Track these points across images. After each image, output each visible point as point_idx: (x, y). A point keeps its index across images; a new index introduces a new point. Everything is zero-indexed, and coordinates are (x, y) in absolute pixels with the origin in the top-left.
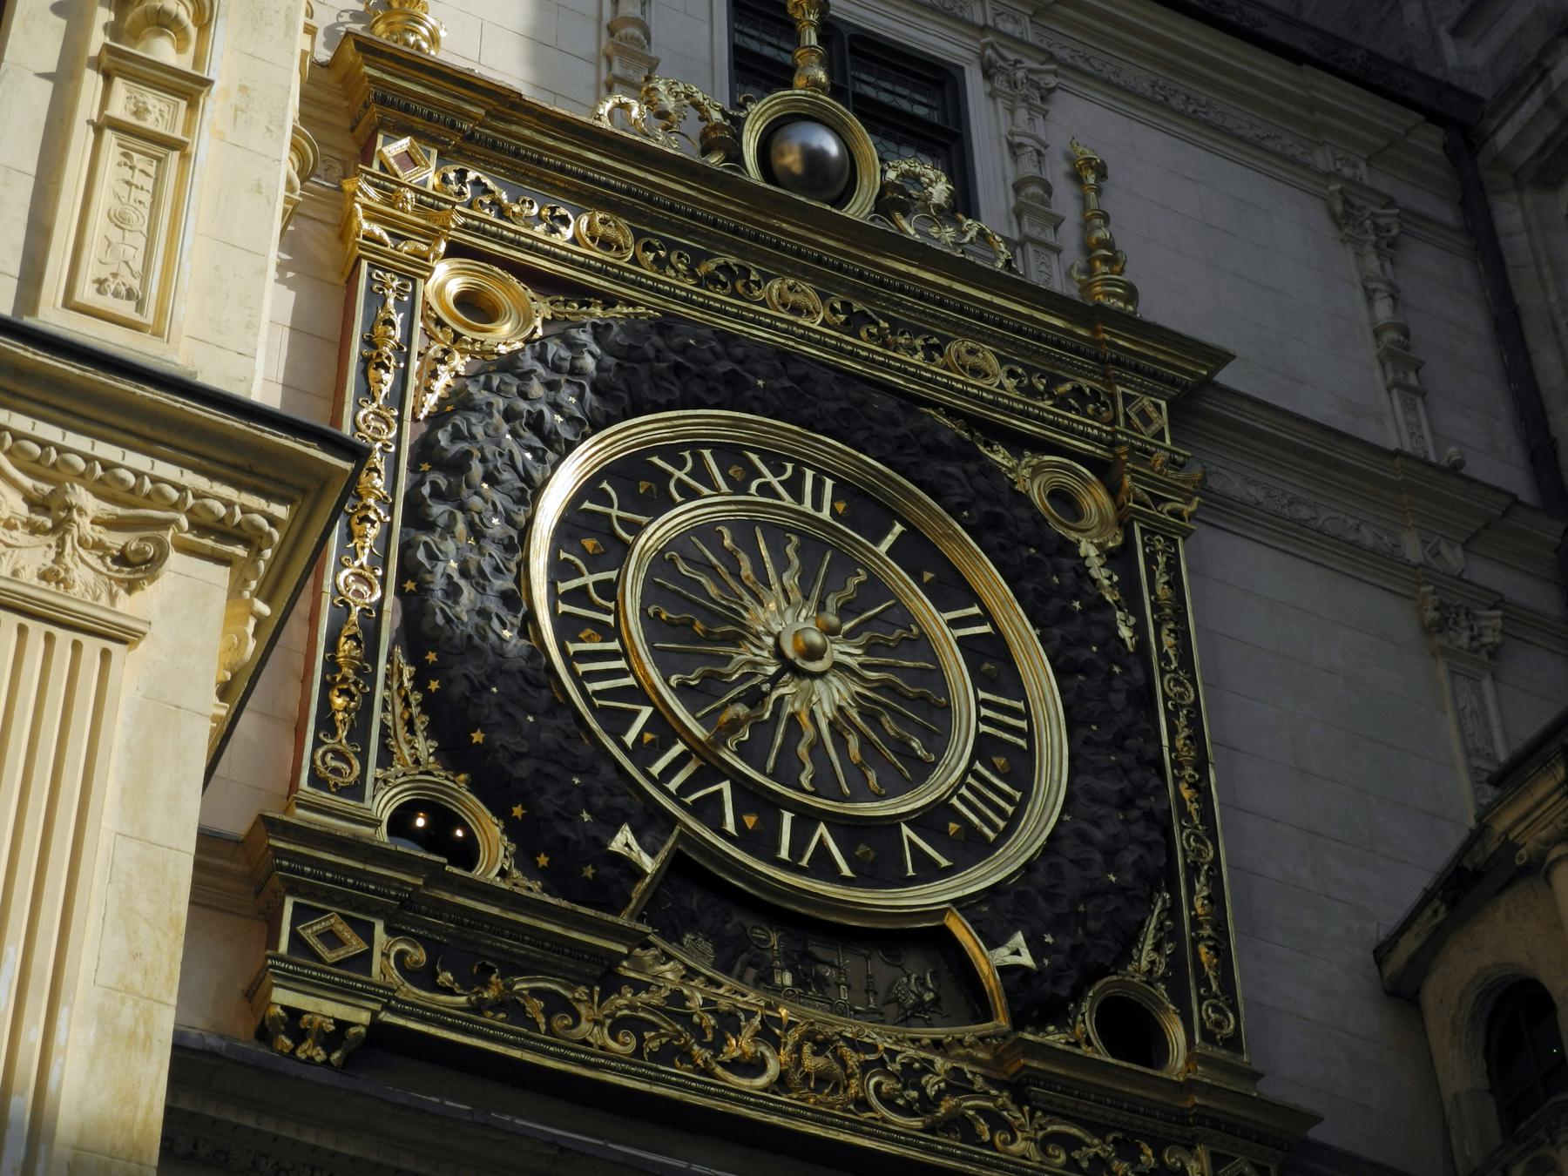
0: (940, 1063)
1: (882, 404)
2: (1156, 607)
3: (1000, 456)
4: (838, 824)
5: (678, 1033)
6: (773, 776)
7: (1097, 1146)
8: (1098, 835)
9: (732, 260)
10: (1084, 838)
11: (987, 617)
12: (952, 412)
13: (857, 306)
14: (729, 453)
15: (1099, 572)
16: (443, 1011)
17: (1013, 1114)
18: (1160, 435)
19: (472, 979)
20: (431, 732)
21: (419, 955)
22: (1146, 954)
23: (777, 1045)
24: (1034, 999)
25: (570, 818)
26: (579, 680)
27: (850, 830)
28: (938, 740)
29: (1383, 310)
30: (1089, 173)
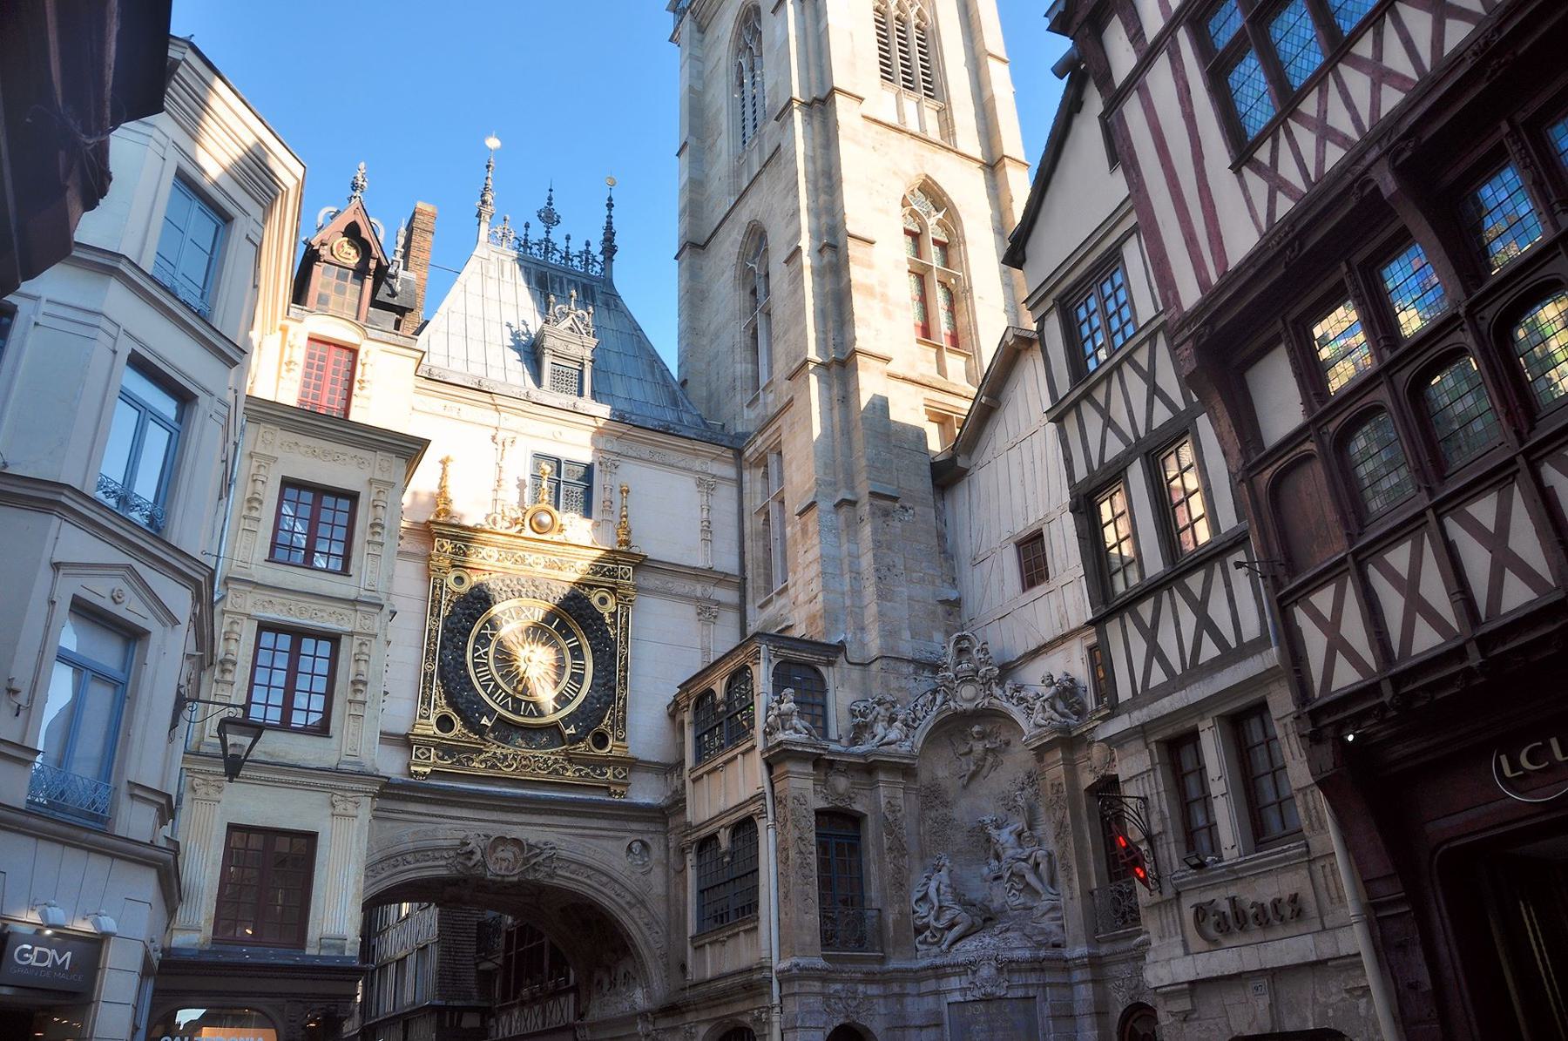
15: (608, 621)
24: (574, 740)
30: (625, 492)
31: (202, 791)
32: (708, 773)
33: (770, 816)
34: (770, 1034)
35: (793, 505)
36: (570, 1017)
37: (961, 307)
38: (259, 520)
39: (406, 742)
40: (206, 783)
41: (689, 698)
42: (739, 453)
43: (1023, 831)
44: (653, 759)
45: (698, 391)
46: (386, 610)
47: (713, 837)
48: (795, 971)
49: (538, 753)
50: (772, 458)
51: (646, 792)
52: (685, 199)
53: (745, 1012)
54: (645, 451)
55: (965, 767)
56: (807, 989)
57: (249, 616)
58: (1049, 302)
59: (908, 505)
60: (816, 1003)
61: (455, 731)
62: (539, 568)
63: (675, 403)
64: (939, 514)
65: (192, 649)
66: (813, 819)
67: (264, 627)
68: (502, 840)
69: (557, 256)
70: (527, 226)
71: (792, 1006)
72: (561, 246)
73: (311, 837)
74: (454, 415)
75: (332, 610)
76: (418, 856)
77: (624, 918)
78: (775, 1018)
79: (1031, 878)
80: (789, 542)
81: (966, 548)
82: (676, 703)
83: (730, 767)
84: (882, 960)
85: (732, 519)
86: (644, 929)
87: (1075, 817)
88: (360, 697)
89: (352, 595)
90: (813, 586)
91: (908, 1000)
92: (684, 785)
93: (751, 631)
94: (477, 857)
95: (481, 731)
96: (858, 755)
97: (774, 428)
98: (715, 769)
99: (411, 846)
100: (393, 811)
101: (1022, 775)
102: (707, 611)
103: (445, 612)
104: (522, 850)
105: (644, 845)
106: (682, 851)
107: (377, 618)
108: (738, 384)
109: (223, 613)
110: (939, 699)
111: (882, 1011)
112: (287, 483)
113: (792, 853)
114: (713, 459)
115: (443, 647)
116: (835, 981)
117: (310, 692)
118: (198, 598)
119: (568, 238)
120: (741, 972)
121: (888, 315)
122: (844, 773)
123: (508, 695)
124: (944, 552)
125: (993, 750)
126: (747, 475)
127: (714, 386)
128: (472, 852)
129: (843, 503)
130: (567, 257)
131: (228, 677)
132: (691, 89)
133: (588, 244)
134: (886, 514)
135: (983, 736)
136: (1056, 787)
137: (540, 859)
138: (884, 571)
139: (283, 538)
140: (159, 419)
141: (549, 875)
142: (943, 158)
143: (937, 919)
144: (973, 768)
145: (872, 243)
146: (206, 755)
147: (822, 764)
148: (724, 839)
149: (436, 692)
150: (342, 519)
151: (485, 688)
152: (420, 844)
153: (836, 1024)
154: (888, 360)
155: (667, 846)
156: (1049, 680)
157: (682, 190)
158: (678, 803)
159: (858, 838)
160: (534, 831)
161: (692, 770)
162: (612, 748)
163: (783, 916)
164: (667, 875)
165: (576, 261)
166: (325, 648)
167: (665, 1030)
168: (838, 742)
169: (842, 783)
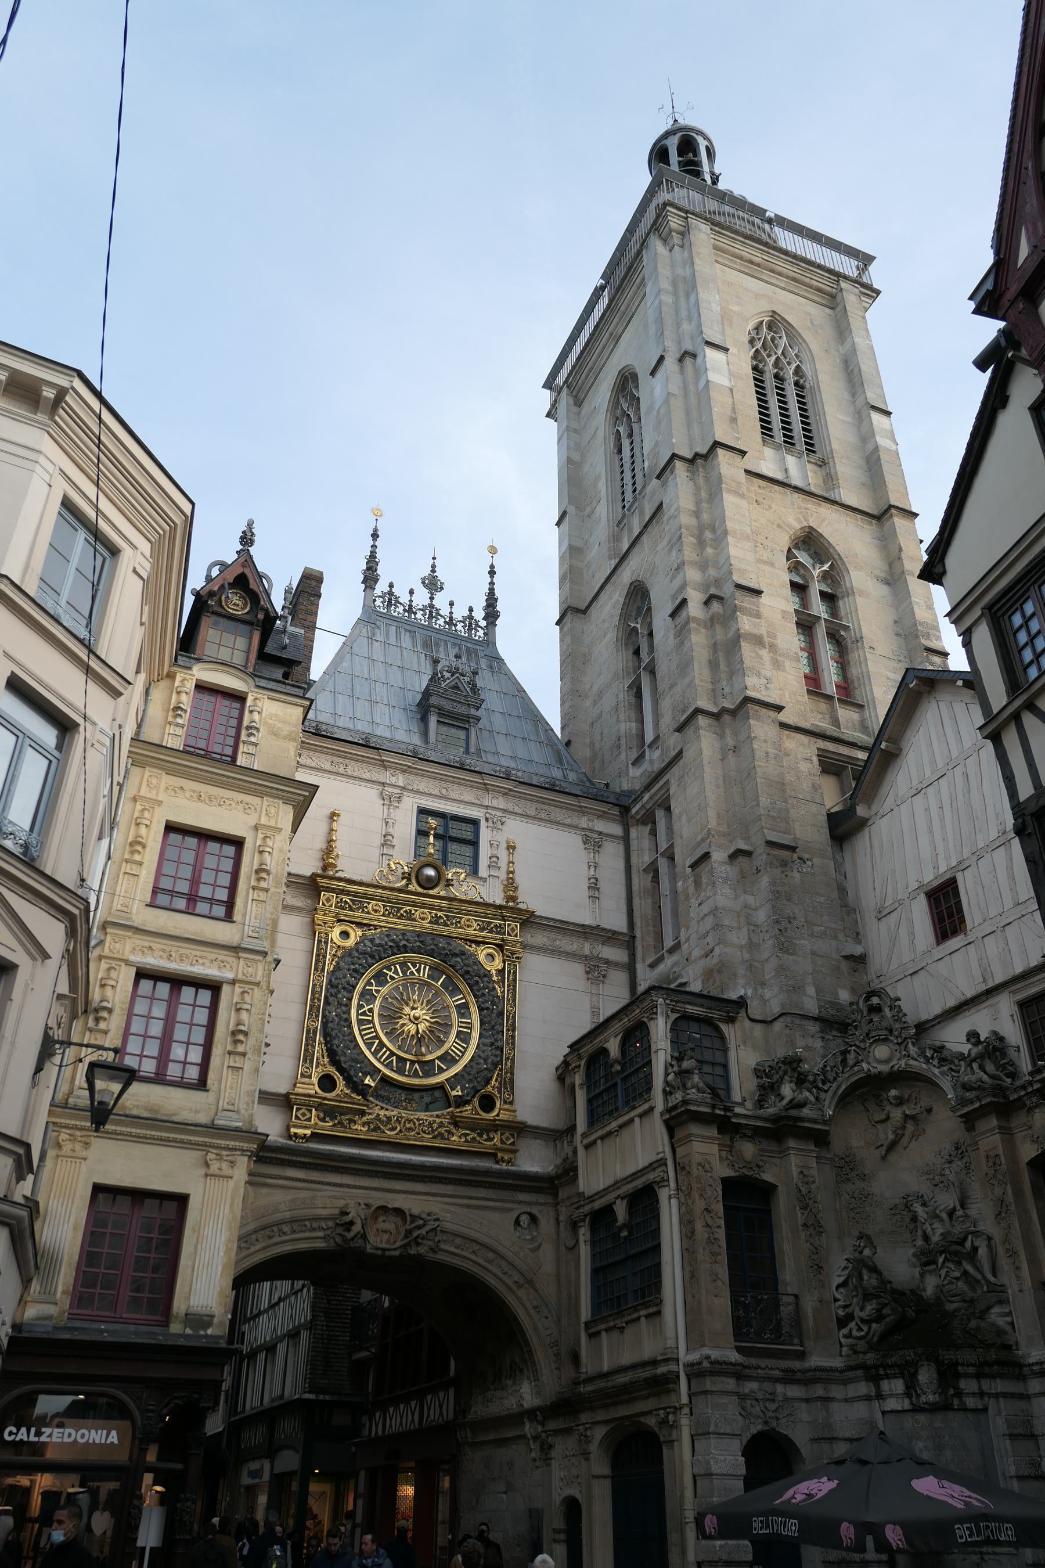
0: (438, 1120)
2: (508, 986)
4: (420, 1062)
5: (376, 1126)
6: (406, 1052)
8: (483, 1055)
9: (408, 908)
10: (480, 1057)
11: (464, 997)
12: (461, 939)
13: (439, 914)
14: (403, 965)
15: (495, 978)
16: (327, 1127)
17: (454, 1131)
18: (516, 936)
19: (332, 1118)
20: (328, 1056)
21: (322, 1115)
22: (493, 1082)
23: (400, 1123)
24: (461, 1102)
25: (357, 1076)
26: (362, 1036)
27: (422, 1063)
28: (447, 1034)
29: (592, 872)
31: (67, 1147)
32: (602, 1138)
33: (673, 1184)
34: (679, 1440)
35: (684, 859)
36: (450, 1412)
37: (853, 657)
38: (141, 864)
39: (285, 1102)
40: (73, 1138)
41: (580, 1058)
42: (625, 810)
43: (954, 1210)
44: (541, 1124)
45: (582, 751)
46: (269, 958)
47: (608, 1210)
48: (706, 1364)
49: (422, 1115)
50: (660, 814)
51: (533, 1160)
52: (566, 566)
53: (649, 1413)
54: (531, 809)
55: (882, 1136)
56: (718, 1387)
57: (127, 963)
58: (977, 612)
59: (806, 856)
60: (732, 1405)
61: (337, 1091)
62: (425, 923)
63: (560, 760)
64: (839, 867)
65: (64, 988)
66: (719, 1188)
67: (142, 974)
68: (383, 1209)
69: (441, 621)
70: (411, 592)
72: (445, 611)
73: (181, 1200)
74: (341, 770)
75: (214, 956)
76: (295, 1226)
77: (511, 1300)
78: (684, 1421)
80: (681, 897)
81: (869, 901)
82: (566, 1063)
83: (625, 1132)
84: (802, 1355)
85: (621, 877)
86: (533, 1312)
87: (1018, 1193)
88: (240, 1048)
89: (235, 940)
91: (834, 1406)
92: (575, 1152)
93: (641, 988)
94: (357, 1228)
96: (766, 1120)
97: (661, 783)
99: (288, 1215)
100: (270, 1177)
101: (948, 1147)
102: (596, 970)
103: (329, 966)
104: (404, 1220)
105: (534, 1219)
106: (574, 1226)
107: (260, 966)
108: (623, 742)
109: (100, 958)
110: (851, 1058)
112: (171, 828)
113: (699, 1226)
114: (599, 817)
115: (327, 1002)
116: (750, 1378)
117: (188, 1043)
118: (71, 933)
119: (451, 604)
120: (644, 1364)
121: (777, 665)
122: (751, 1138)
123: (392, 1054)
124: (846, 905)
125: (913, 1117)
126: (633, 833)
127: (597, 746)
128: (352, 1223)
129: (736, 855)
130: (451, 622)
131: (102, 1025)
132: (569, 460)
133: (471, 610)
134: (784, 864)
135: (900, 1102)
136: (994, 1160)
137: (423, 1231)
138: (784, 924)
139: (166, 883)
140: (38, 747)
141: (432, 1249)
142: (827, 512)
143: (862, 1309)
144: (891, 1137)
145: (758, 593)
146: (75, 1108)
148: (621, 1210)
150: (228, 865)
151: (369, 1046)
152: (298, 1213)
153: (754, 1430)
154: (779, 708)
155: (557, 1219)
156: (973, 1036)
157: (562, 558)
158: (569, 1172)
159: (769, 1212)
161: (584, 1135)
162: (499, 1112)
165: (460, 627)
166: (205, 997)
167: (557, 1432)
168: (742, 1105)
169: (748, 1149)
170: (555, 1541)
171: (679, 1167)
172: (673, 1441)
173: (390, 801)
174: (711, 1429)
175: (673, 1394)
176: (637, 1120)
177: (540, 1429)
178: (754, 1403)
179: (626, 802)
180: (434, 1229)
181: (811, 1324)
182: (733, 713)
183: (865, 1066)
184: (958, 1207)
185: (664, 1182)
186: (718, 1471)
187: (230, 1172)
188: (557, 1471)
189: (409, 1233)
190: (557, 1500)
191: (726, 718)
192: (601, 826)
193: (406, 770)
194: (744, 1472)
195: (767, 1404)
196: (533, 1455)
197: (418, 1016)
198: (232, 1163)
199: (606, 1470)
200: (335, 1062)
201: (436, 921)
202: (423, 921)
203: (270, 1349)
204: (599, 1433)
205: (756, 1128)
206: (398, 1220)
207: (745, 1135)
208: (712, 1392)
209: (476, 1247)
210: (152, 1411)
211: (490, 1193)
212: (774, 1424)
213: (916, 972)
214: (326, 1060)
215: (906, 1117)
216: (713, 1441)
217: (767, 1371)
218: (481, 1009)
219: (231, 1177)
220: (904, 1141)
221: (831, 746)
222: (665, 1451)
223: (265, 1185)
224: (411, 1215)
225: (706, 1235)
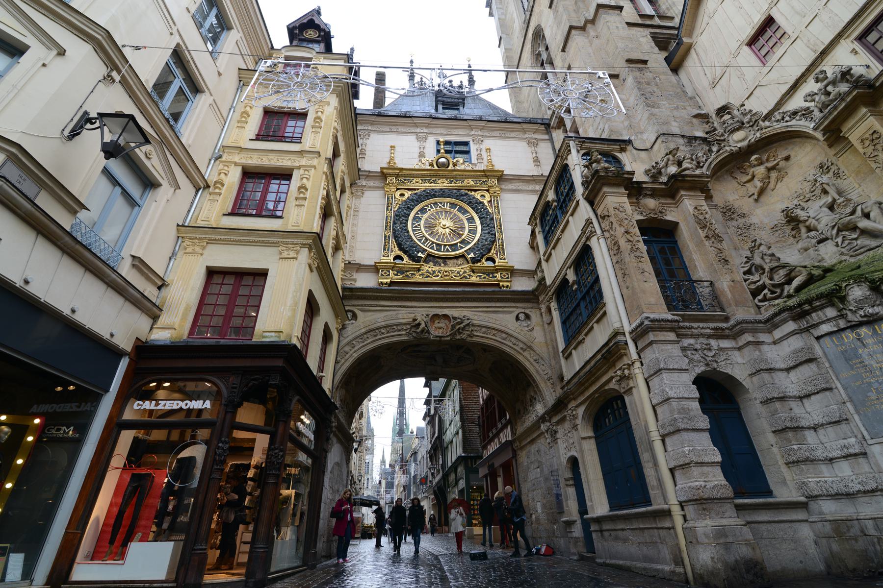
1: (455, 191)
3: (473, 193)
7: (484, 276)
16: (399, 278)
24: (475, 261)
27: (451, 246)
33: (599, 231)
34: (636, 386)
41: (535, 219)
42: (549, 125)
47: (565, 281)
48: (646, 322)
54: (497, 134)
56: (663, 338)
57: (236, 164)
68: (436, 316)
71: (649, 355)
77: (520, 358)
78: (637, 369)
79: (863, 224)
86: (534, 363)
90: (601, 126)
91: (765, 348)
94: (423, 325)
95: (417, 260)
98: (558, 239)
99: (383, 324)
104: (450, 321)
105: (528, 317)
111: (740, 360)
113: (622, 242)
114: (534, 133)
115: (394, 223)
123: (433, 243)
125: (773, 168)
128: (419, 324)
134: (640, 70)
137: (462, 326)
141: (469, 335)
147: (635, 190)
148: (571, 277)
149: (392, 243)
151: (420, 240)
160: (456, 311)
163: (625, 291)
164: (544, 330)
167: (558, 423)
170: (567, 485)
171: (602, 218)
172: (631, 388)
173: (422, 139)
174: (662, 366)
175: (625, 358)
176: (571, 218)
177: (548, 424)
178: (694, 352)
179: (547, 122)
180: (468, 325)
181: (730, 296)
182: (593, 21)
183: (728, 148)
184: (837, 197)
185: (593, 233)
186: (675, 396)
187: (295, 256)
188: (561, 445)
189: (453, 327)
190: (564, 461)
191: (589, 26)
192: (536, 136)
193: (428, 126)
194: (697, 395)
195: (705, 352)
196: (548, 441)
197: (445, 224)
198: (298, 252)
199: (591, 433)
200: (401, 249)
201: (451, 182)
202: (442, 183)
203: (452, 442)
204: (581, 411)
205: (654, 189)
206: (447, 321)
207: (646, 195)
208: (656, 342)
209: (494, 332)
210: (235, 388)
211: (498, 304)
212: (715, 365)
213: (752, 93)
214: (397, 249)
215: (769, 170)
216: (665, 375)
217: (699, 330)
218: (480, 218)
219: (296, 259)
220: (772, 185)
221: (658, 31)
222: (626, 398)
223: (369, 311)
224: (454, 318)
225: (629, 247)
